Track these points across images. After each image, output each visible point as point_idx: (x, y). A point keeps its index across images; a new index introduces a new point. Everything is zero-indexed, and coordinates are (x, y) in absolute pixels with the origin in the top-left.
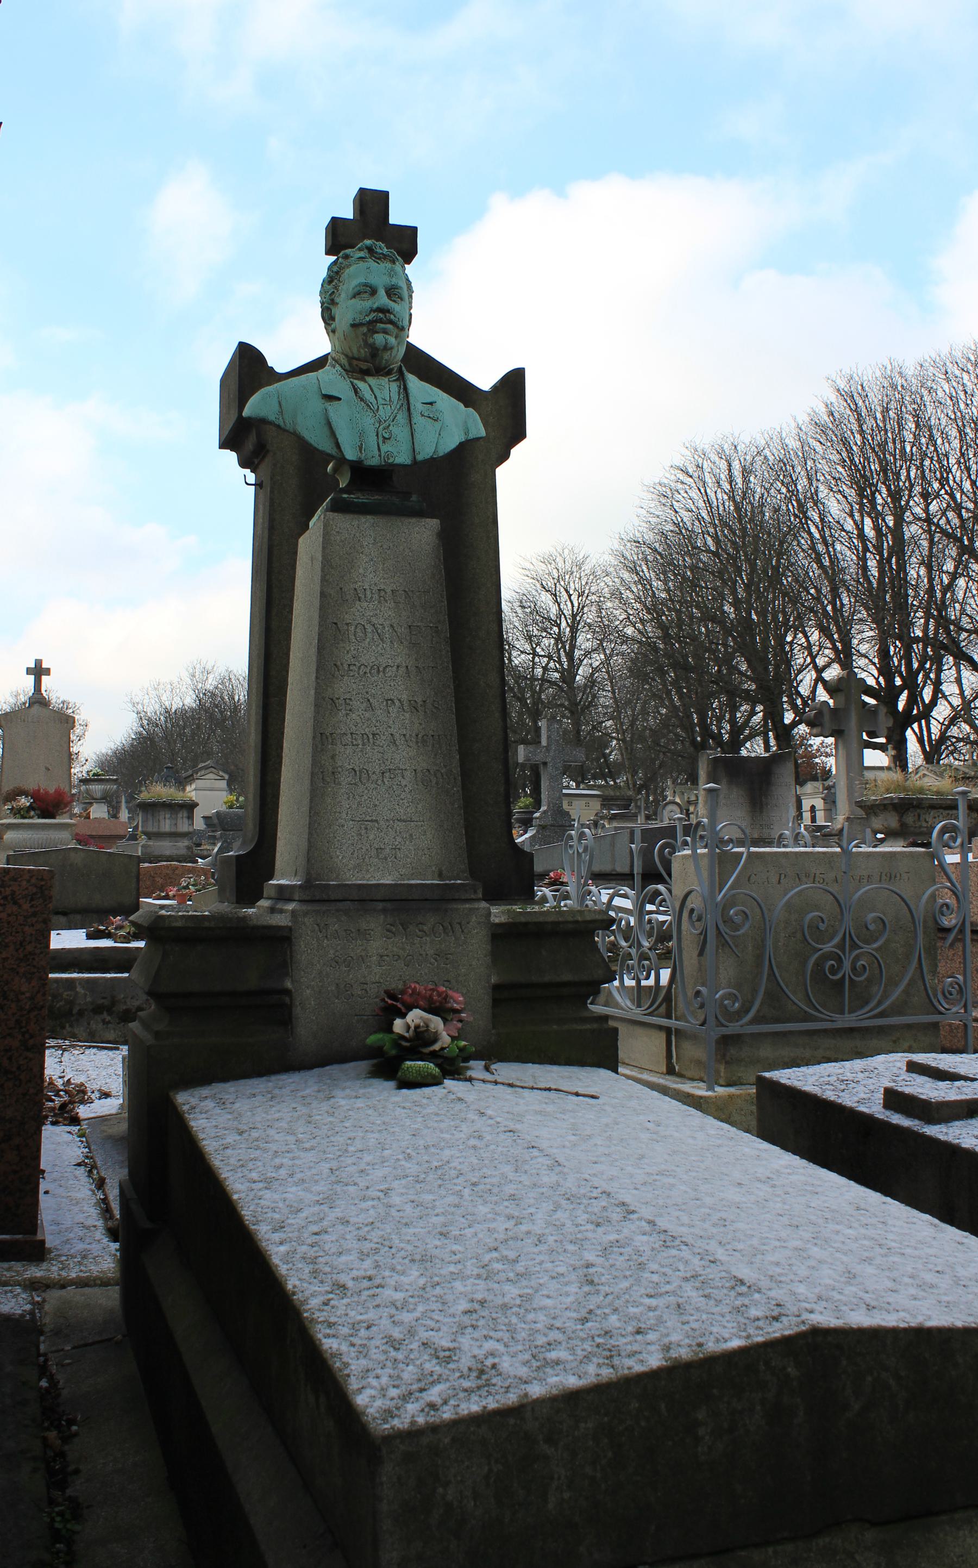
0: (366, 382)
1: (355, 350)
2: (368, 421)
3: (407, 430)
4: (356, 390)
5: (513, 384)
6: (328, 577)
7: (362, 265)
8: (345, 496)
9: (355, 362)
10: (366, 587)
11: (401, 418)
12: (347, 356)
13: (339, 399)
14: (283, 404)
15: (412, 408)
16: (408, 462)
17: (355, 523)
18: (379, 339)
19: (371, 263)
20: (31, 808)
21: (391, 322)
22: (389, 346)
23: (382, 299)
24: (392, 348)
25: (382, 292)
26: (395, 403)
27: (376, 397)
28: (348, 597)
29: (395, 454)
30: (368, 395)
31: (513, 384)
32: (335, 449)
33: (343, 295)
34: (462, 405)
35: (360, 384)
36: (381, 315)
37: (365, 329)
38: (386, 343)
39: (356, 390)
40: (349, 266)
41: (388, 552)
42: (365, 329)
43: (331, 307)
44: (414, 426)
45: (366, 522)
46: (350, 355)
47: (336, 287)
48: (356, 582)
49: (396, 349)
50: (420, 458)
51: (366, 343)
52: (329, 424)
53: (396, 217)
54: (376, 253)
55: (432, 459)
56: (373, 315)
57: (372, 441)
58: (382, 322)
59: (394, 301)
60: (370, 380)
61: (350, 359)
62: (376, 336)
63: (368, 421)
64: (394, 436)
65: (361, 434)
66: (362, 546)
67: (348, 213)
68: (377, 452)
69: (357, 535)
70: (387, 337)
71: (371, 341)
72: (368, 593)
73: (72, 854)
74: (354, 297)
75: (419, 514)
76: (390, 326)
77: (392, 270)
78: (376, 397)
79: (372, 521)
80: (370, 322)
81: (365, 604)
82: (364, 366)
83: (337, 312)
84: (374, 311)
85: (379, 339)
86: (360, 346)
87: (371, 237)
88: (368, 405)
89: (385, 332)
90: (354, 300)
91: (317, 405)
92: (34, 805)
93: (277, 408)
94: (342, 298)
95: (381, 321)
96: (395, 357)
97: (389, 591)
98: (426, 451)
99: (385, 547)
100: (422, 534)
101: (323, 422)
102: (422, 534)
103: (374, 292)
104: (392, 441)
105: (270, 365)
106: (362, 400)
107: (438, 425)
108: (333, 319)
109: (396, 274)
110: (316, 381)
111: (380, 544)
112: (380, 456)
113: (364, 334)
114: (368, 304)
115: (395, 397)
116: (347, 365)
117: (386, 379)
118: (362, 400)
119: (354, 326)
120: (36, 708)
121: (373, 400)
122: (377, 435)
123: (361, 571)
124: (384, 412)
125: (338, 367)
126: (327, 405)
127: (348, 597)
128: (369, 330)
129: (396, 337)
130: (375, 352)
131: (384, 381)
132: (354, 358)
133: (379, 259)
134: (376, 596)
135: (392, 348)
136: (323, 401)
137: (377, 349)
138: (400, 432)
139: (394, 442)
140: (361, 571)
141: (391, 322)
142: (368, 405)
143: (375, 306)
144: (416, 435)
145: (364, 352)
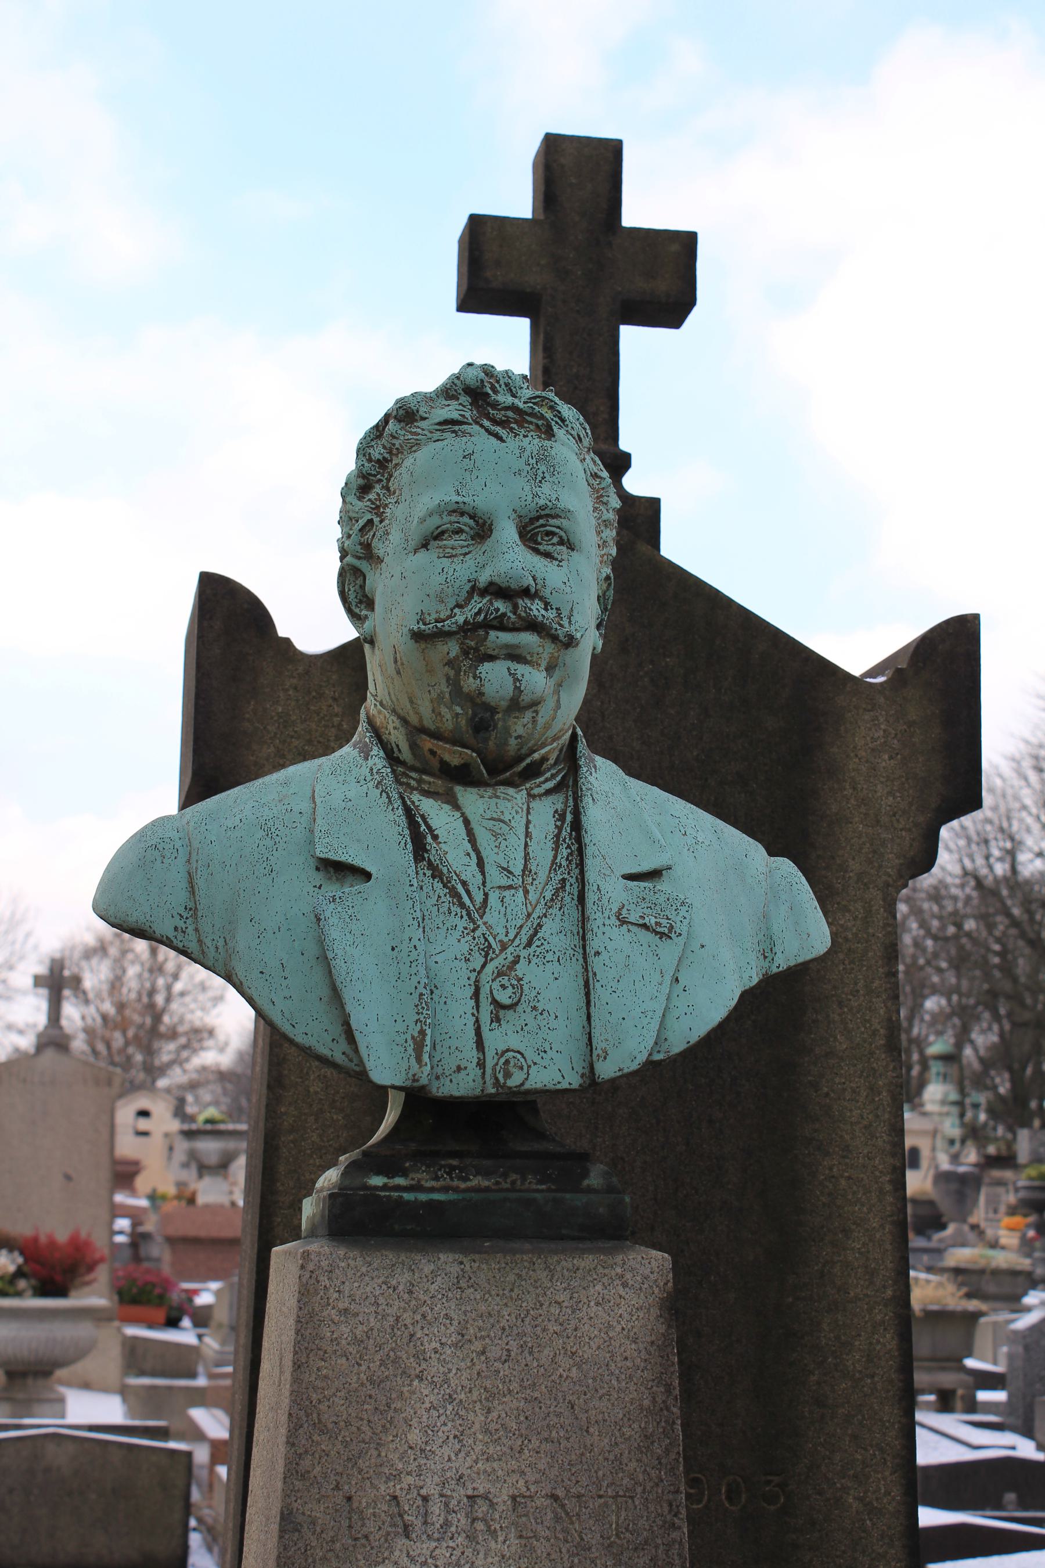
0: (457, 807)
1: (425, 708)
2: (450, 948)
3: (570, 972)
4: (419, 839)
5: (949, 656)
6: (306, 1463)
7: (452, 445)
8: (377, 1181)
9: (427, 744)
10: (431, 1488)
11: (556, 933)
12: (405, 721)
13: (367, 876)
14: (200, 883)
15: (591, 897)
16: (572, 1080)
17: (402, 1278)
18: (495, 678)
19: (480, 440)
20: (19, 1273)
21: (533, 626)
22: (526, 698)
23: (510, 558)
24: (535, 704)
25: (507, 532)
26: (542, 876)
27: (481, 864)
28: (371, 1526)
29: (530, 1055)
30: (454, 852)
31: (949, 656)
32: (344, 1045)
33: (395, 536)
34: (756, 851)
35: (438, 815)
36: (501, 606)
37: (453, 648)
38: (518, 690)
39: (419, 839)
40: (415, 446)
41: (505, 1370)
42: (453, 648)
43: (364, 565)
44: (596, 963)
45: (436, 1271)
46: (413, 719)
47: (378, 509)
48: (397, 1477)
49: (550, 703)
50: (606, 1070)
51: (457, 691)
52: (324, 961)
53: (642, 209)
54: (495, 405)
55: (650, 1065)
56: (478, 603)
57: (457, 1015)
58: (503, 628)
59: (548, 555)
60: (470, 798)
61: (416, 731)
62: (486, 668)
63: (450, 948)
64: (529, 994)
65: (427, 996)
66: (420, 1356)
67: (516, 199)
68: (471, 1054)
69: (407, 1317)
70: (521, 669)
71: (469, 684)
72: (436, 1508)
73: (51, 1447)
74: (425, 546)
75: (608, 1231)
76: (528, 639)
77: (543, 457)
78: (481, 864)
79: (455, 1269)
80: (468, 629)
81: (424, 1548)
82: (454, 756)
83: (380, 583)
84: (483, 592)
85: (495, 678)
86: (441, 696)
87: (579, 265)
88: (454, 893)
89: (515, 655)
90: (422, 554)
91: (297, 889)
92: (26, 1269)
93: (180, 897)
94: (392, 543)
95: (501, 625)
96: (547, 726)
97: (502, 1497)
98: (626, 1051)
99: (494, 1352)
100: (612, 1305)
101: (312, 950)
102: (612, 1305)
103: (482, 530)
104: (524, 1015)
105: (282, 633)
106: (436, 873)
107: (670, 951)
108: (370, 604)
109: (553, 470)
110: (305, 806)
111: (478, 1346)
112: (481, 1064)
113: (450, 663)
114: (467, 568)
115: (542, 854)
116: (404, 746)
117: (520, 796)
118: (436, 873)
119: (418, 636)
120: (50, 1054)
121: (471, 873)
122: (476, 995)
123: (415, 1436)
124: (504, 916)
125: (378, 759)
126: (332, 889)
127: (371, 1526)
128: (465, 652)
129: (550, 669)
130: (483, 717)
131: (511, 802)
132: (422, 730)
133: (503, 423)
134: (460, 1520)
135: (535, 704)
136: (318, 878)
137: (493, 710)
138: (550, 981)
139: (529, 1017)
140: (415, 1436)
141: (533, 626)
142: (454, 893)
143: (484, 579)
144: (600, 994)
145: (452, 717)
